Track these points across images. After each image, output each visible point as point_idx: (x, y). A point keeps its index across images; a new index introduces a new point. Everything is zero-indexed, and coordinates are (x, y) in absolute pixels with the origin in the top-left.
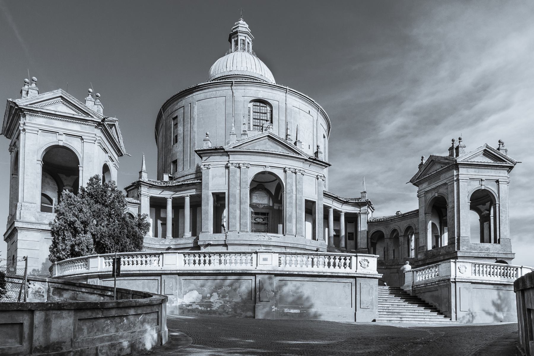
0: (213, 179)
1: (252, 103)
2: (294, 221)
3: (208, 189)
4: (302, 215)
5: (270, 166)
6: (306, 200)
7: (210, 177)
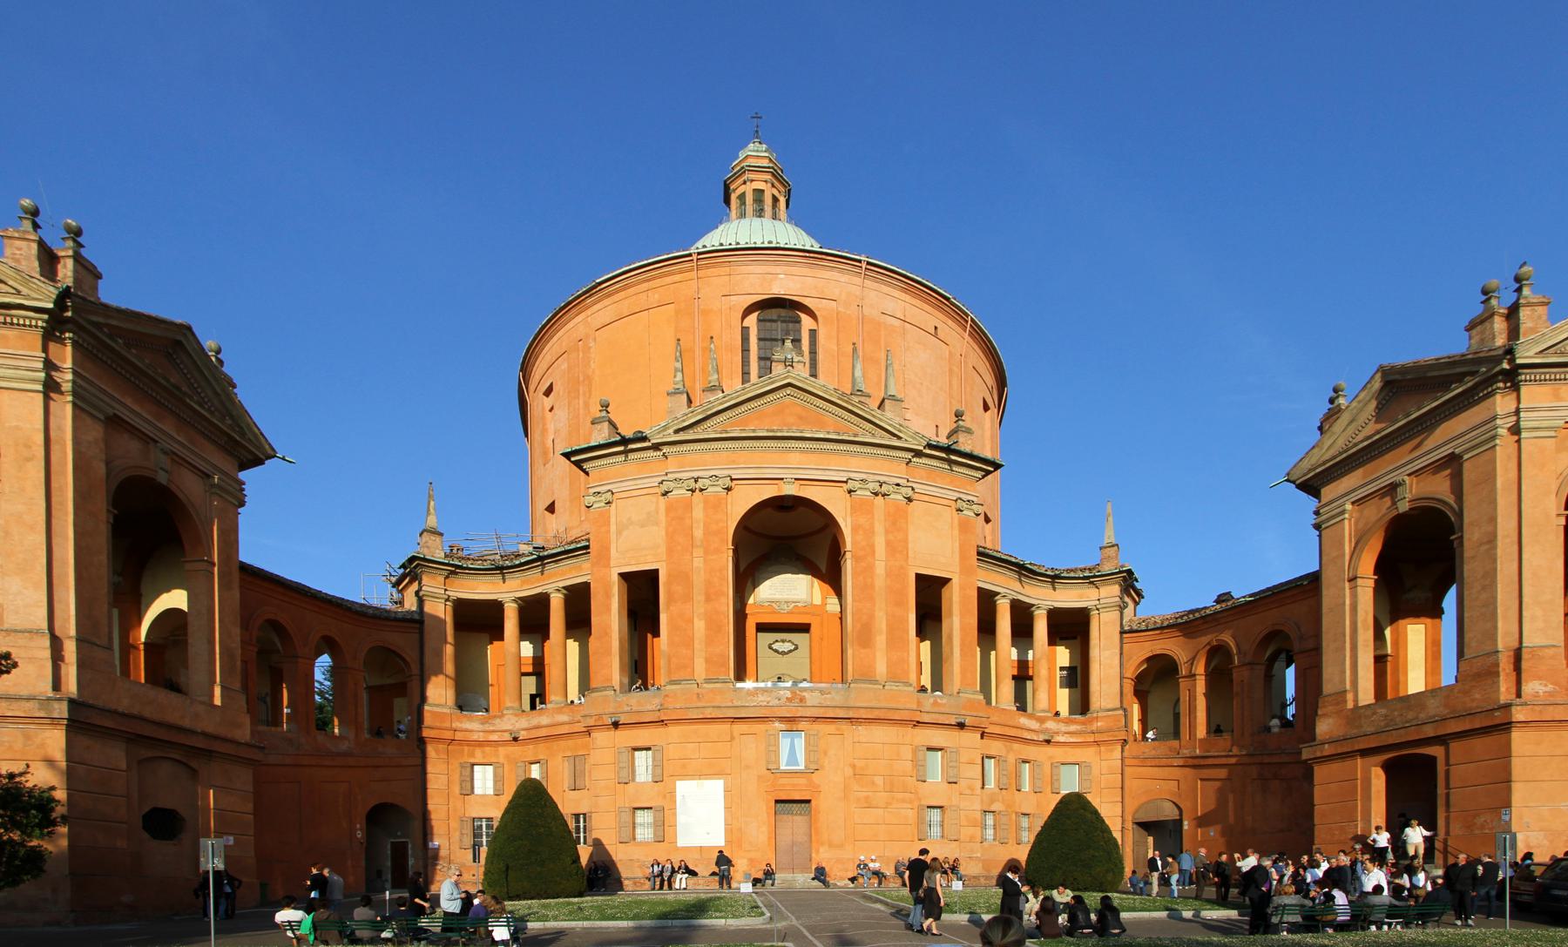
0: (619, 533)
1: (754, 317)
2: (881, 640)
3: (608, 566)
4: (907, 621)
5: (795, 479)
6: (917, 575)
7: (613, 528)
